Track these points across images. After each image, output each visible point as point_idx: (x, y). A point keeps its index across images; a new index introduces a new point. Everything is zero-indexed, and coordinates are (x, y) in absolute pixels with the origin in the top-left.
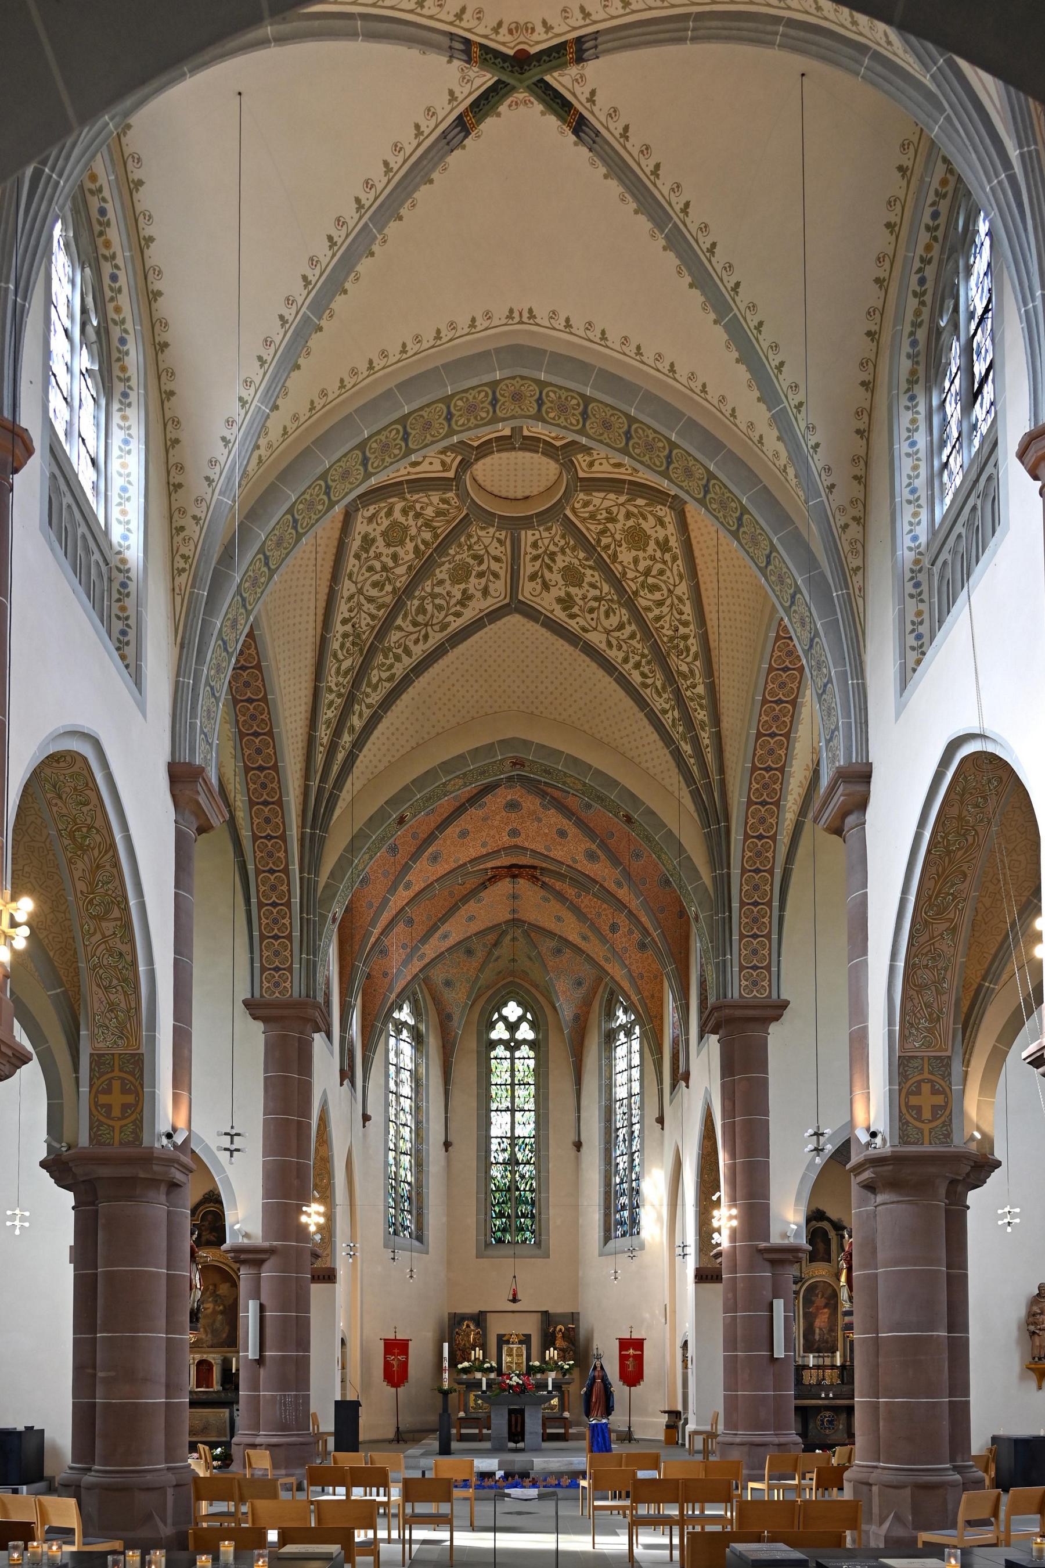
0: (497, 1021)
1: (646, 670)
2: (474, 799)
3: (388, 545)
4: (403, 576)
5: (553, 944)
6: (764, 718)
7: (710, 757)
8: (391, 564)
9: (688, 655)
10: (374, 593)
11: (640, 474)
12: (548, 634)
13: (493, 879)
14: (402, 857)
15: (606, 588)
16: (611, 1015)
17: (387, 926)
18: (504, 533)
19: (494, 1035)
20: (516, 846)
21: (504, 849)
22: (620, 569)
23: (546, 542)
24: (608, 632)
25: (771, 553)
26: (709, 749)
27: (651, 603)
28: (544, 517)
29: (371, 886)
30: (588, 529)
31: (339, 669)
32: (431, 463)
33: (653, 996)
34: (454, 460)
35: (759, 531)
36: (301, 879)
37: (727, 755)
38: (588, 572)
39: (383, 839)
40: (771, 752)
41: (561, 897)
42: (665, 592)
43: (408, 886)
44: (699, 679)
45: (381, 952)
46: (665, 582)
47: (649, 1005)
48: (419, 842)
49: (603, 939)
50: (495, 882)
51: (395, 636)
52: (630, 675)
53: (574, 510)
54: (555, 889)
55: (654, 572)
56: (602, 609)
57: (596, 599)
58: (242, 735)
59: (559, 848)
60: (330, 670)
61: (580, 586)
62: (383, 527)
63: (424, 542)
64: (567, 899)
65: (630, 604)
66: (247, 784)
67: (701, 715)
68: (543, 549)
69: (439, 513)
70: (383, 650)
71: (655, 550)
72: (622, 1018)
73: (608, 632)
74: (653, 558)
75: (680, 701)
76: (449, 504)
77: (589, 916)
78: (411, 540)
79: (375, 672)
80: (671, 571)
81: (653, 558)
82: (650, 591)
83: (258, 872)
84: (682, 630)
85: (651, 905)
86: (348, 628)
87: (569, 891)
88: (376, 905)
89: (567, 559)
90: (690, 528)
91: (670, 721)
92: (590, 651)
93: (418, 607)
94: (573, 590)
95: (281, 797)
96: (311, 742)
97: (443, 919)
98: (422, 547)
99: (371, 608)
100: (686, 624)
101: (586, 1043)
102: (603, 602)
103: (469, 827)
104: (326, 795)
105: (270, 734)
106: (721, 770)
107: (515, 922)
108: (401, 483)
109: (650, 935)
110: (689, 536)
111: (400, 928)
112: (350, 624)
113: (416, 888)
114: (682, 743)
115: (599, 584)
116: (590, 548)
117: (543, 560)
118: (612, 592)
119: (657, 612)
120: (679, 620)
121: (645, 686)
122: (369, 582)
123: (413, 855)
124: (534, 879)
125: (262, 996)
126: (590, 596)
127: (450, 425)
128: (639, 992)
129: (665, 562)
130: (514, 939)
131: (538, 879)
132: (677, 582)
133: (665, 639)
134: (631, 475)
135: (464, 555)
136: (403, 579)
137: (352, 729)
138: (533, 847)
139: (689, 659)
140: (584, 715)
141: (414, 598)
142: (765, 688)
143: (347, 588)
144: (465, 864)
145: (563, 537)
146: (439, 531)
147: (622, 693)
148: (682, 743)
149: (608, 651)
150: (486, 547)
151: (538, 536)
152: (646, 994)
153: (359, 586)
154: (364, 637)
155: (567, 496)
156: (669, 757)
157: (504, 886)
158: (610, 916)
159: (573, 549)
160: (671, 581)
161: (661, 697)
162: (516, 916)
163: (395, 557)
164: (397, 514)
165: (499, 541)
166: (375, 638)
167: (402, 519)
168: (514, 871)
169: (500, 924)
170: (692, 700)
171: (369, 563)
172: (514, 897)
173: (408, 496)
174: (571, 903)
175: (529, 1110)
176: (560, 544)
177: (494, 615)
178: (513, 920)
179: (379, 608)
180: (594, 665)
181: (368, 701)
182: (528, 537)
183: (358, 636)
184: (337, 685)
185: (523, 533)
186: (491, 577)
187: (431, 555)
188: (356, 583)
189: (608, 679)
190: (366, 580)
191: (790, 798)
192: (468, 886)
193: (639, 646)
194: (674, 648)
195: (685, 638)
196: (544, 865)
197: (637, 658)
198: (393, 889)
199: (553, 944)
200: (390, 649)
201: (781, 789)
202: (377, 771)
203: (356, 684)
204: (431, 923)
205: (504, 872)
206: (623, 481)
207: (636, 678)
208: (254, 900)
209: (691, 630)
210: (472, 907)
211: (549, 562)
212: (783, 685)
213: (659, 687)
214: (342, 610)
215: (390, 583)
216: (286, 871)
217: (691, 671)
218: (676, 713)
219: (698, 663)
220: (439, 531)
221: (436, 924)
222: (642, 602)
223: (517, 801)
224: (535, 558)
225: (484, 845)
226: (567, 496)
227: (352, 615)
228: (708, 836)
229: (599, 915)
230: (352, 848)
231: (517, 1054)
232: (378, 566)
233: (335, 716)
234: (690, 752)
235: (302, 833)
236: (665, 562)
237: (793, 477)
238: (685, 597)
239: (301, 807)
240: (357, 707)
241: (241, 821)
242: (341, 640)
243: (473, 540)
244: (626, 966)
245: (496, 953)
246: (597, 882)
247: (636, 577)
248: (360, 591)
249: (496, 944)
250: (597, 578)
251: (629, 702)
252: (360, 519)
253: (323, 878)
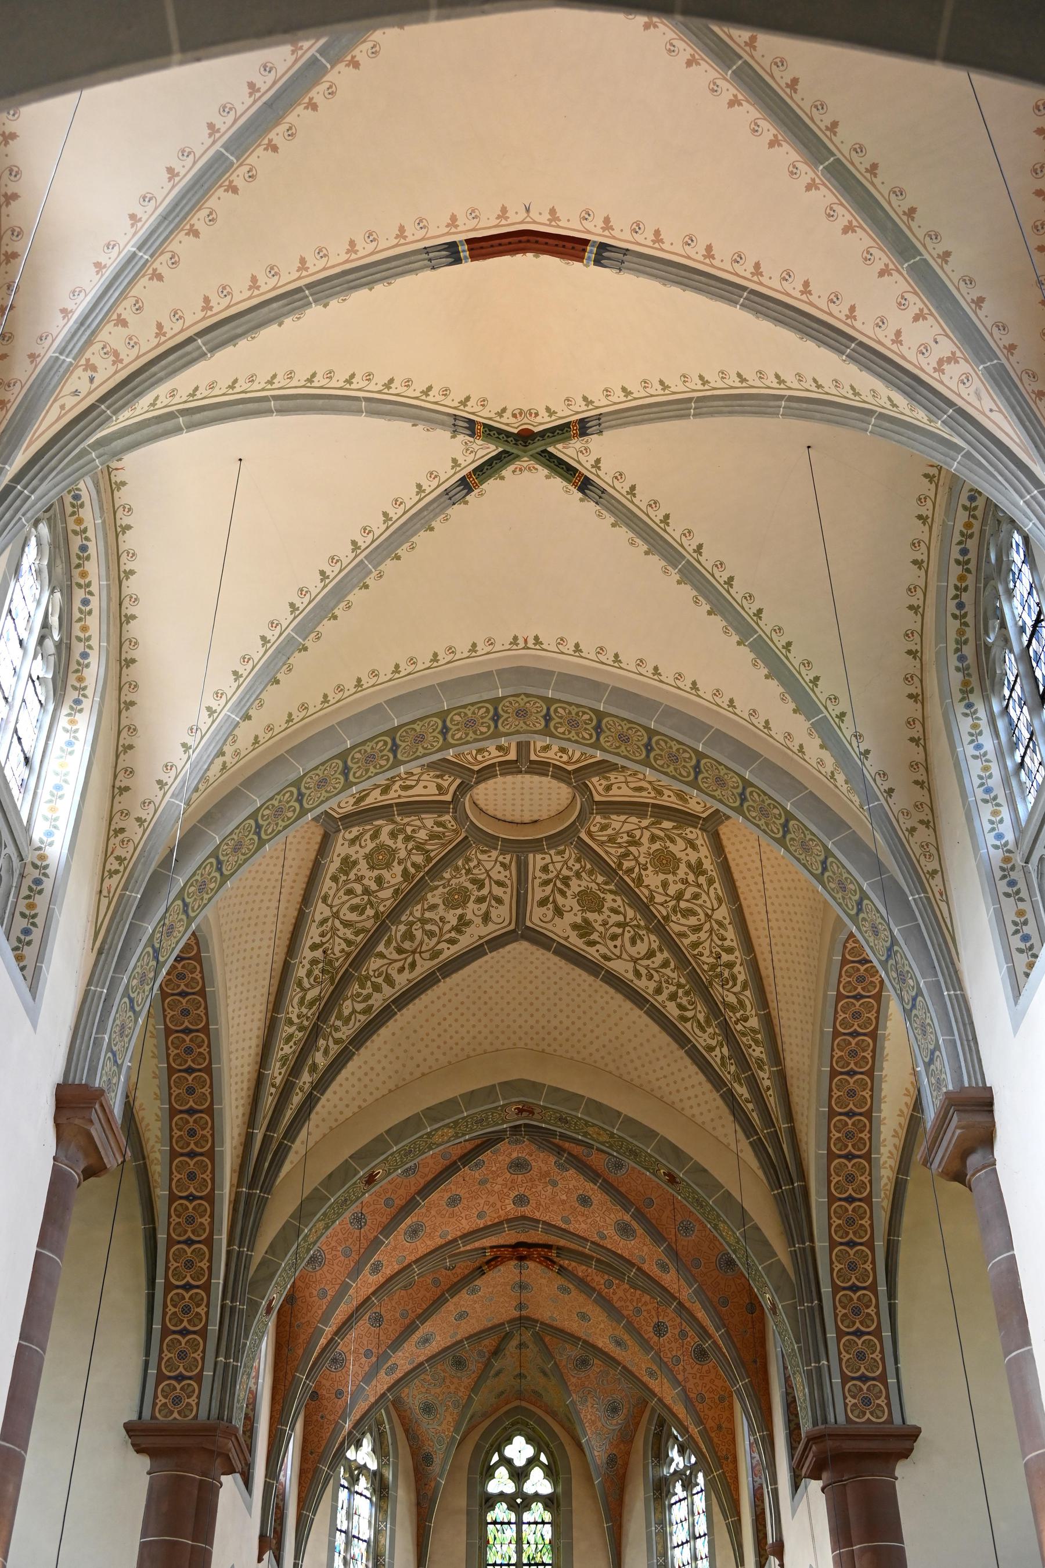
1: (684, 1001)
2: (468, 1158)
3: (372, 868)
4: (388, 899)
5: (575, 1352)
6: (838, 1053)
7: (772, 1100)
8: (374, 887)
9: (735, 985)
10: (353, 917)
11: (665, 797)
12: (562, 963)
13: (494, 1262)
14: (369, 1231)
15: (630, 913)
16: (661, 1457)
17: (344, 1324)
18: (508, 857)
19: (493, 1487)
20: (524, 1218)
21: (508, 1221)
22: (647, 892)
23: (558, 866)
24: (635, 961)
25: (826, 858)
26: (770, 1092)
27: (685, 929)
28: (553, 840)
29: (325, 1268)
30: (607, 852)
31: (303, 998)
32: (425, 787)
33: (719, 1427)
34: (451, 783)
35: (809, 837)
36: (229, 1253)
37: (795, 1099)
38: (609, 897)
39: (345, 1203)
40: (852, 1093)
41: (584, 1285)
42: (702, 917)
43: (376, 1268)
44: (750, 1010)
45: (335, 1361)
46: (701, 906)
47: (716, 1440)
48: (393, 1210)
49: (645, 1345)
50: (496, 1266)
51: (374, 964)
52: (664, 1007)
53: (589, 833)
54: (576, 1276)
55: (687, 896)
56: (627, 936)
57: (618, 925)
58: (171, 1071)
59: (581, 1219)
60: (291, 1000)
61: (600, 912)
62: (367, 850)
63: (414, 865)
64: (594, 1289)
65: (660, 928)
66: (171, 1130)
67: (758, 1052)
70: (359, 979)
71: (686, 874)
72: (678, 1461)
73: (635, 961)
74: (684, 881)
75: (728, 1035)
77: (625, 1313)
78: (399, 863)
79: (348, 1002)
80: (708, 894)
81: (684, 881)
82: (683, 916)
83: (170, 1242)
84: (725, 957)
85: (709, 1294)
86: (318, 954)
87: (597, 1279)
88: (331, 1293)
89: (584, 883)
90: (727, 850)
91: (718, 1060)
92: (614, 980)
93: (405, 933)
94: (591, 916)
95: (213, 1146)
96: (259, 1081)
97: (424, 1316)
98: (412, 870)
99: (349, 934)
100: (730, 951)
101: (627, 1498)
102: (627, 928)
103: (462, 1192)
104: (274, 1146)
105: (208, 1070)
106: (790, 1117)
107: (523, 1322)
108: (391, 806)
109: (710, 1337)
110: (726, 858)
111: (363, 1327)
112: (321, 950)
113: (388, 1271)
114: (735, 1085)
115: (622, 909)
116: (610, 872)
117: (555, 884)
118: (639, 917)
119: (693, 938)
120: (721, 947)
121: (685, 1019)
122: (348, 905)
123: (384, 1228)
124: (549, 1262)
125: (153, 1417)
127: (445, 739)
128: (700, 1421)
129: (699, 886)
130: (521, 1345)
131: (554, 1263)
132: (716, 906)
133: (706, 967)
134: (655, 798)
135: (462, 880)
136: (388, 903)
137: (314, 1068)
138: (546, 1219)
139: (735, 990)
140: (610, 1053)
141: (401, 922)
142: (835, 1019)
144: (455, 1240)
145: (578, 860)
147: (655, 1028)
148: (735, 1085)
149: (636, 981)
150: (487, 872)
151: (548, 860)
152: (710, 1424)
155: (582, 818)
156: (720, 1102)
157: (507, 1272)
158: (653, 1313)
159: (591, 873)
160: (709, 905)
161: (705, 1032)
162: (524, 1313)
163: (379, 880)
164: (384, 837)
165: (503, 865)
166: (350, 965)
168: (521, 1251)
169: (503, 1324)
170: (744, 1034)
172: (522, 1286)
173: (398, 819)
174: (600, 1294)
176: (574, 869)
177: (496, 943)
178: (521, 1318)
180: (619, 997)
181: (337, 1035)
182: (536, 861)
183: (330, 963)
184: (299, 1017)
185: (531, 856)
186: (493, 903)
187: (423, 877)
189: (638, 1012)
190: (343, 903)
191: (883, 1150)
192: (459, 1271)
193: (675, 975)
194: (717, 976)
195: (730, 965)
196: (562, 1243)
197: (673, 988)
198: (355, 1272)
199: (575, 1352)
200: (368, 978)
201: (870, 1139)
202: (342, 1118)
203: (323, 1015)
204: (407, 1321)
205: (507, 1253)
206: (647, 805)
207: (672, 1010)
208: (160, 1281)
209: (737, 956)
210: (464, 1299)
211: (562, 887)
212: (857, 1015)
213: (702, 1021)
215: (372, 906)
216: (209, 1242)
217: (741, 1003)
218: (725, 1050)
219: (748, 993)
220: (432, 854)
221: (413, 1322)
222: (674, 928)
223: (525, 1160)
224: (546, 883)
225: (480, 1216)
226: (582, 818)
227: (324, 940)
228: (780, 1200)
229: (639, 1311)
230: (302, 1214)
231: (527, 1517)
232: (359, 889)
233: (294, 1052)
234: (746, 1095)
235: (237, 1193)
236: (699, 886)
237: (843, 783)
238: (726, 922)
239: (239, 1161)
240: (322, 1042)
241: (156, 1177)
242: (308, 966)
243: (472, 865)
244: (680, 1384)
245: (497, 1365)
246: (633, 1265)
247: (666, 902)
249: (496, 1352)
250: (619, 902)
251: (664, 1038)
252: (340, 841)
253: (259, 1254)
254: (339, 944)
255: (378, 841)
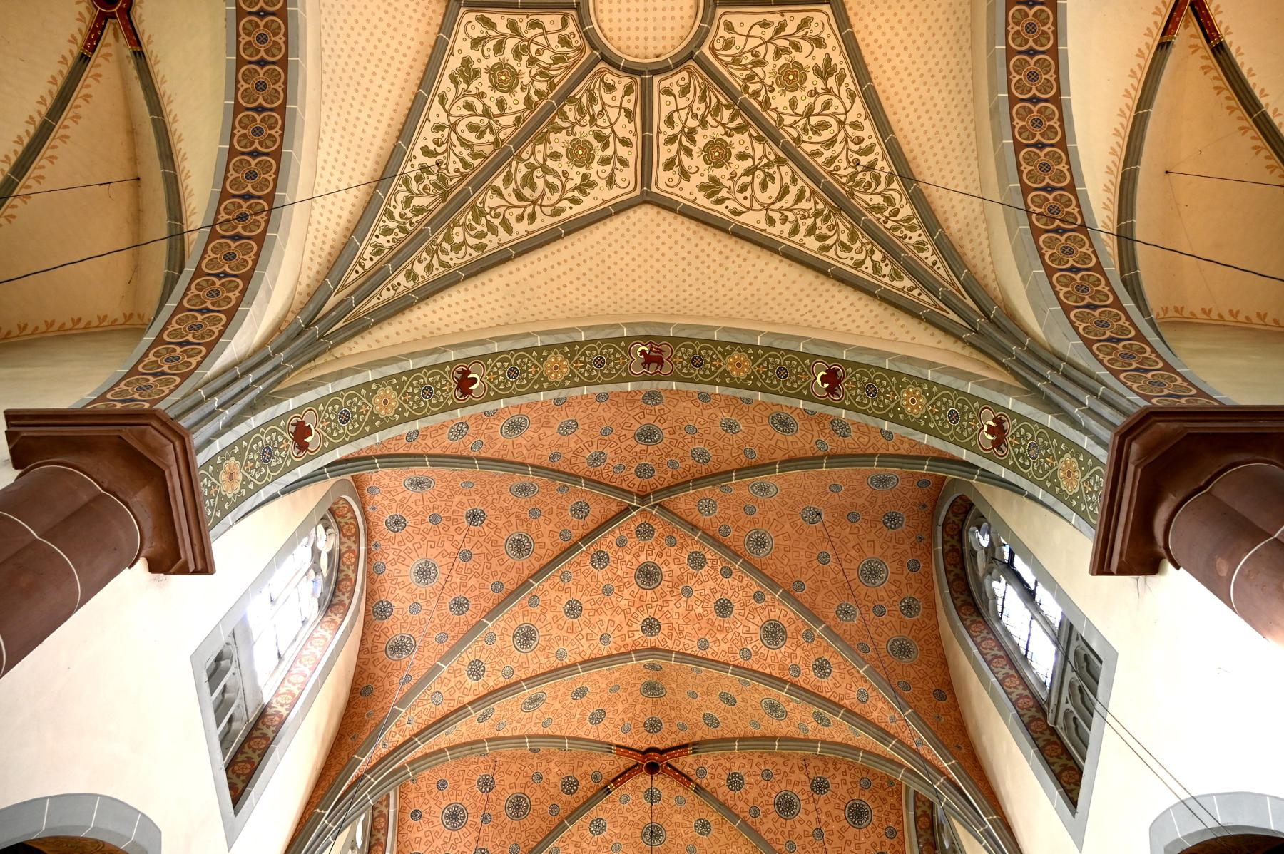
4: (509, 127)
8: (495, 110)
10: (471, 137)
63: (537, 92)
68: (681, 126)
69: (558, 59)
76: (569, 46)
98: (535, 98)
99: (466, 154)
126: (739, 172)
136: (509, 131)
143: (436, 113)
146: (556, 81)
153: (453, 120)
154: (450, 183)
163: (501, 103)
164: (508, 54)
167: (513, 63)
171: (470, 99)
179: (475, 157)
188: (449, 115)
190: (462, 117)
214: (426, 136)
215: (492, 132)
224: (671, 140)
232: (479, 108)
243: (598, 108)
248: (453, 127)
254: (455, 162)
255: (502, 57)
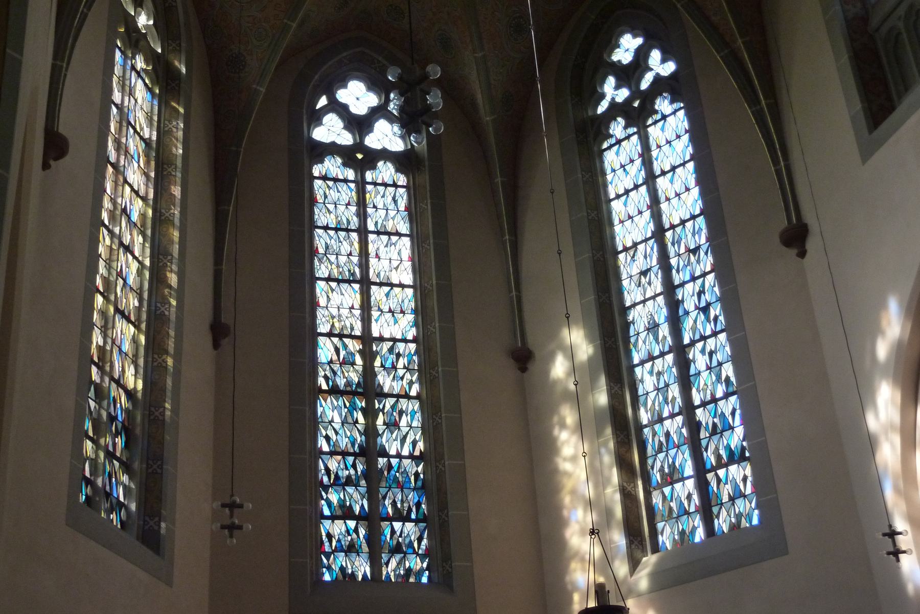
0: (326, 110)
175: (402, 286)
